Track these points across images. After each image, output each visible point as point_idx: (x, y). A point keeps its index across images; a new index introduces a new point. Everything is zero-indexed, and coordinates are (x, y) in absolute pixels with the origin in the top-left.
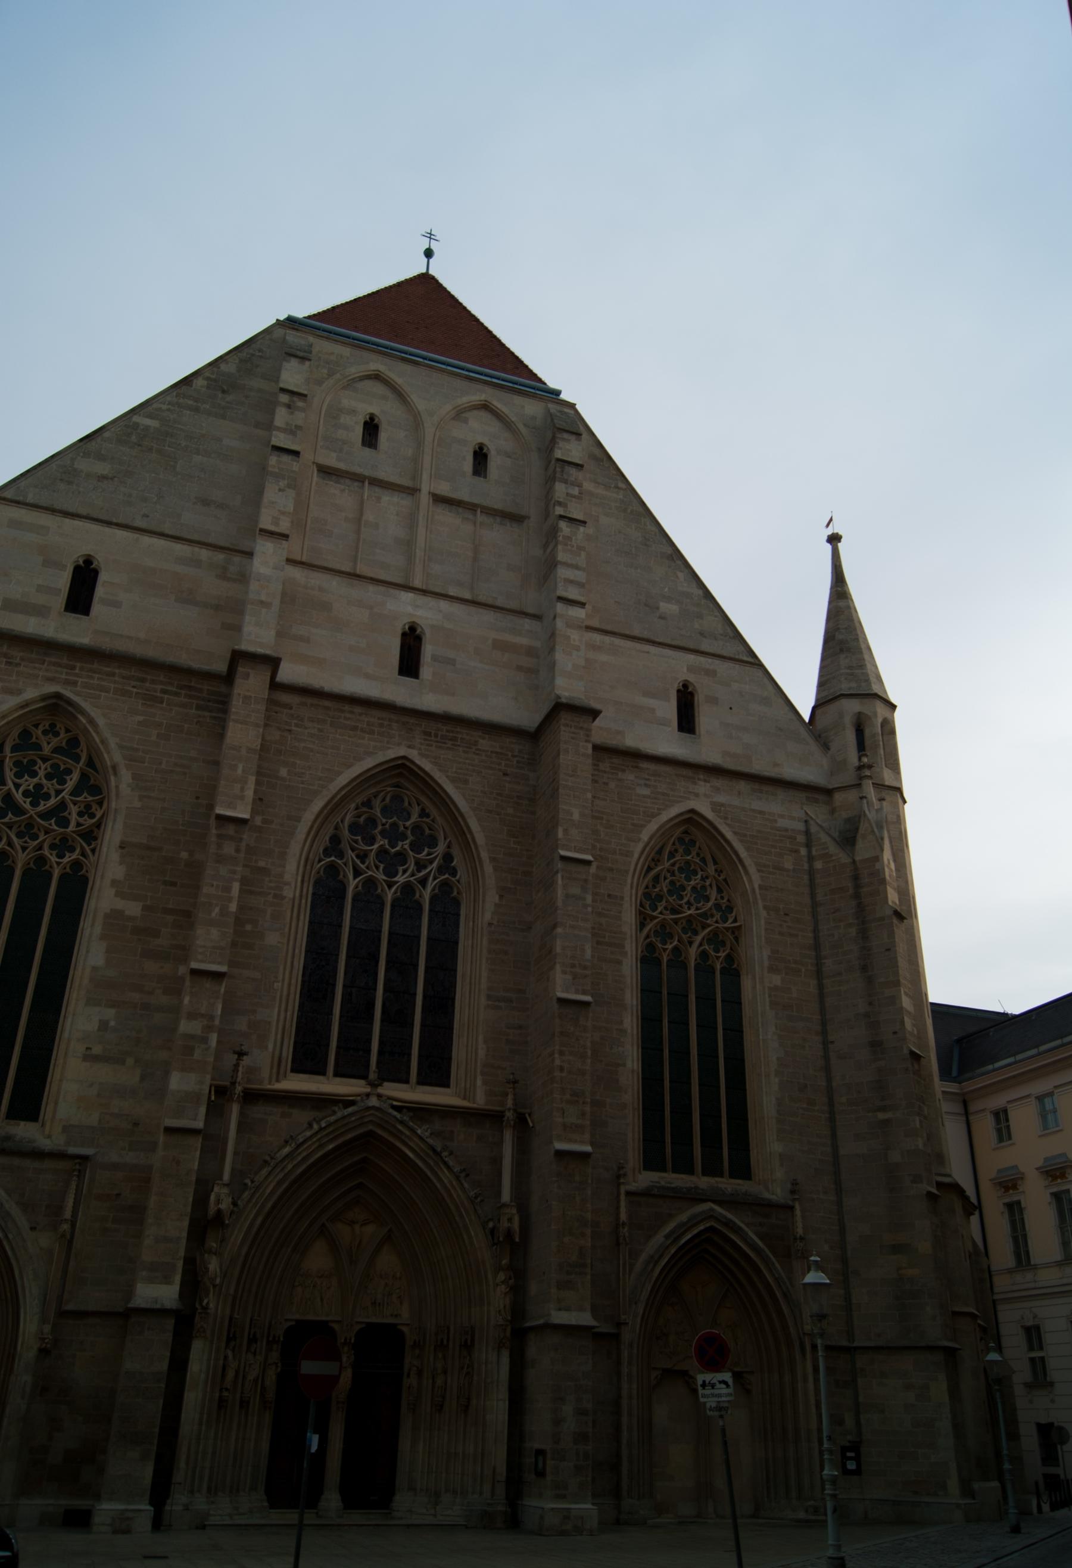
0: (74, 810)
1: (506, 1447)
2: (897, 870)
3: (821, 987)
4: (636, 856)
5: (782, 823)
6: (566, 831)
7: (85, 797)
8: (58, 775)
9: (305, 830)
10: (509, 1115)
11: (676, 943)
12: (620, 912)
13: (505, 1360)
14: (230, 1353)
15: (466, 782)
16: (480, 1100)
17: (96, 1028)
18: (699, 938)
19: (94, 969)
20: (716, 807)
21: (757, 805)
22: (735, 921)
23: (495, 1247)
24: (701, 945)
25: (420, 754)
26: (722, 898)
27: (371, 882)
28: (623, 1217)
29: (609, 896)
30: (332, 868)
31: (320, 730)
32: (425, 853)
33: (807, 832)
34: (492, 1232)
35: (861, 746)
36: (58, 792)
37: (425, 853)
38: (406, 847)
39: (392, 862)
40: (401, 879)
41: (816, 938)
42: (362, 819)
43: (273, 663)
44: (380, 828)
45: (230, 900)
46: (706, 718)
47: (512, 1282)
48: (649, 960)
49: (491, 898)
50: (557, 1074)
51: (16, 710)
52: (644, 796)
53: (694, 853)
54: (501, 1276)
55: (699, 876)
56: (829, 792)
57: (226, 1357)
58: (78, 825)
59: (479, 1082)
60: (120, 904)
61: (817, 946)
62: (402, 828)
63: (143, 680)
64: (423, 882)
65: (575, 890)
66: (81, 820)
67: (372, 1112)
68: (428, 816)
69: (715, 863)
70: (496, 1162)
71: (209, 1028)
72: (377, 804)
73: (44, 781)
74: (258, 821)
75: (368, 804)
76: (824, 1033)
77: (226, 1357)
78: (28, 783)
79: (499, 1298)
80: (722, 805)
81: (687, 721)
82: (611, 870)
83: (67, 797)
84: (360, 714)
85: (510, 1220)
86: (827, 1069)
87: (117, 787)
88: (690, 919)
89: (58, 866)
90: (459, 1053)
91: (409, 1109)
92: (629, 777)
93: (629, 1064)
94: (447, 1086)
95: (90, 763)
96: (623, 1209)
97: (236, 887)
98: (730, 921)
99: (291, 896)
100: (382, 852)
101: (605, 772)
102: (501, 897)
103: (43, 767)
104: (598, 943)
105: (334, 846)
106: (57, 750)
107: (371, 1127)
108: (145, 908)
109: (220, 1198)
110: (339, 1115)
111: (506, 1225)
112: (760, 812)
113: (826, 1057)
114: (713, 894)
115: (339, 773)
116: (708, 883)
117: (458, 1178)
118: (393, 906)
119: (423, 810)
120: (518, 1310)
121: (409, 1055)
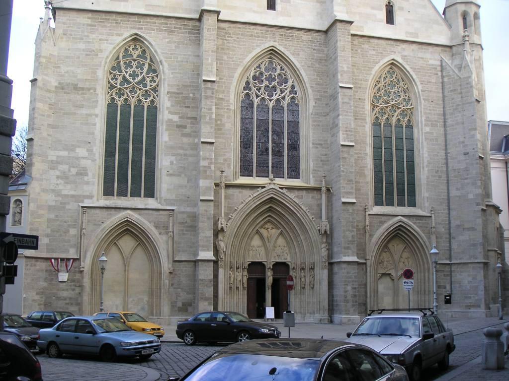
0: (148, 80)
2: (478, 80)
3: (445, 130)
4: (370, 81)
5: (431, 62)
6: (341, 75)
7: (151, 74)
8: (140, 67)
9: (236, 81)
10: (324, 189)
11: (387, 116)
12: (364, 105)
13: (326, 272)
14: (231, 272)
15: (298, 54)
16: (312, 184)
17: (169, 164)
18: (396, 114)
19: (166, 142)
20: (404, 57)
21: (420, 55)
22: (411, 105)
24: (397, 116)
25: (279, 44)
26: (406, 96)
27: (263, 98)
28: (367, 223)
29: (359, 99)
30: (248, 95)
31: (238, 38)
32: (283, 86)
33: (441, 66)
34: (319, 230)
35: (465, 27)
36: (141, 73)
37: (283, 86)
38: (276, 84)
39: (271, 90)
40: (275, 97)
41: (444, 111)
42: (257, 74)
43: (218, 13)
44: (265, 76)
45: (212, 113)
46: (398, 16)
47: (327, 247)
48: (376, 124)
49: (312, 103)
50: (342, 174)
51: (122, 42)
52: (373, 55)
53: (394, 78)
54: (324, 245)
55: (396, 87)
56: (451, 47)
57: (230, 274)
58: (151, 86)
59: (311, 177)
60: (171, 117)
61: (444, 114)
62: (273, 76)
63: (167, 24)
64: (284, 98)
65: (346, 100)
66: (151, 84)
67: (272, 190)
68: (283, 70)
69: (403, 81)
70: (320, 205)
71: (211, 163)
72: (263, 66)
73: (136, 69)
74: (218, 80)
75: (259, 67)
76: (446, 149)
77: (230, 274)
78: (130, 71)
79: (324, 252)
80: (406, 56)
81: (390, 19)
82: (360, 88)
83: (145, 75)
84: (253, 29)
85: (326, 226)
86: (447, 163)
87: (163, 69)
88: (393, 106)
89: (146, 103)
90: (302, 166)
91: (286, 188)
92: (366, 46)
93: (369, 167)
94: (299, 178)
95: (151, 61)
96: (367, 221)
97: (214, 108)
98: (409, 105)
99: (233, 108)
100: (267, 86)
101: (356, 45)
102: (316, 102)
103: (134, 64)
104: (356, 119)
105: (247, 86)
106: (139, 56)
107: (272, 195)
108: (180, 118)
109: (222, 223)
110: (260, 192)
111: (324, 228)
112: (422, 58)
113: (447, 159)
114: (402, 94)
115: (247, 56)
116: (400, 90)
118: (272, 109)
119: (281, 67)
120: (330, 256)
121: (284, 167)
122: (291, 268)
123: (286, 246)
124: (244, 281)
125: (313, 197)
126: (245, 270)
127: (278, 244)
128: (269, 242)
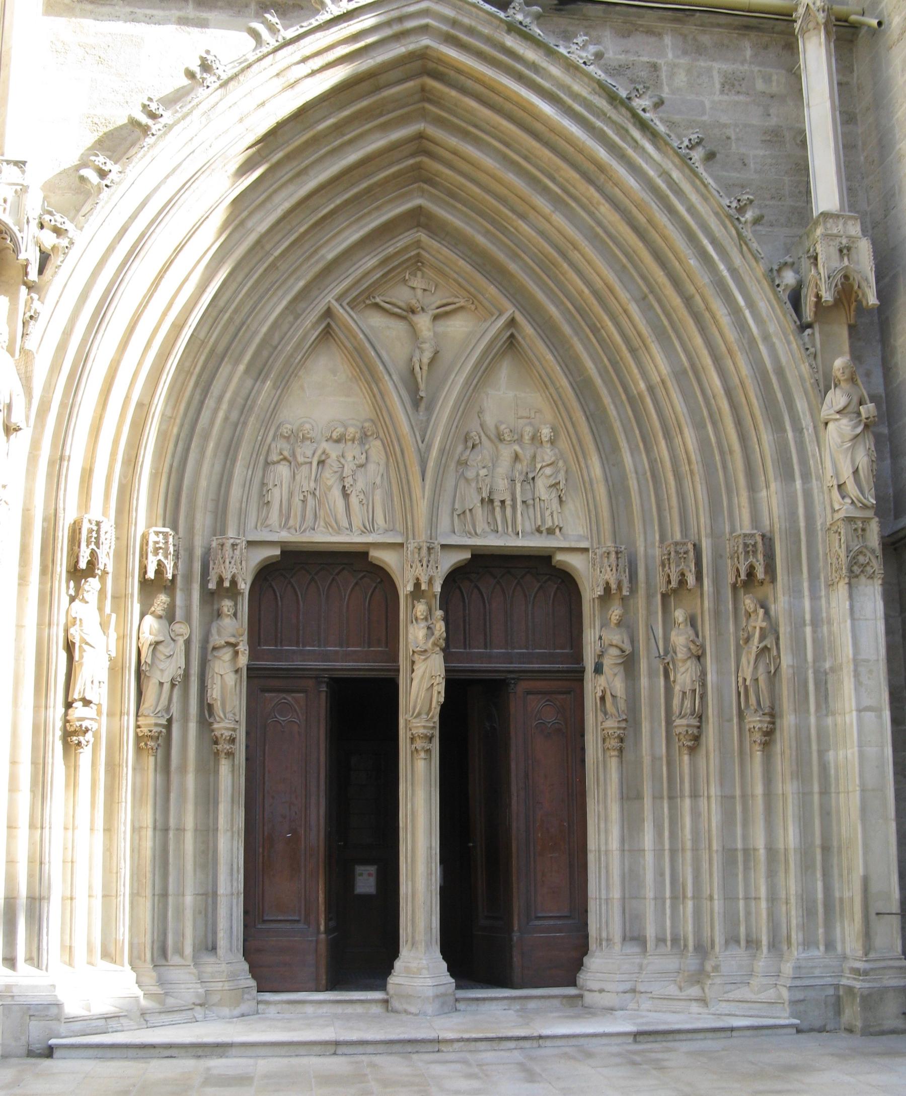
1: (893, 826)
23: (809, 331)
107: (425, 41)
117: (685, 162)
122: (590, 592)
123: (546, 432)
124: (215, 693)
125: (730, 83)
126: (227, 605)
127: (490, 420)
128: (416, 402)
